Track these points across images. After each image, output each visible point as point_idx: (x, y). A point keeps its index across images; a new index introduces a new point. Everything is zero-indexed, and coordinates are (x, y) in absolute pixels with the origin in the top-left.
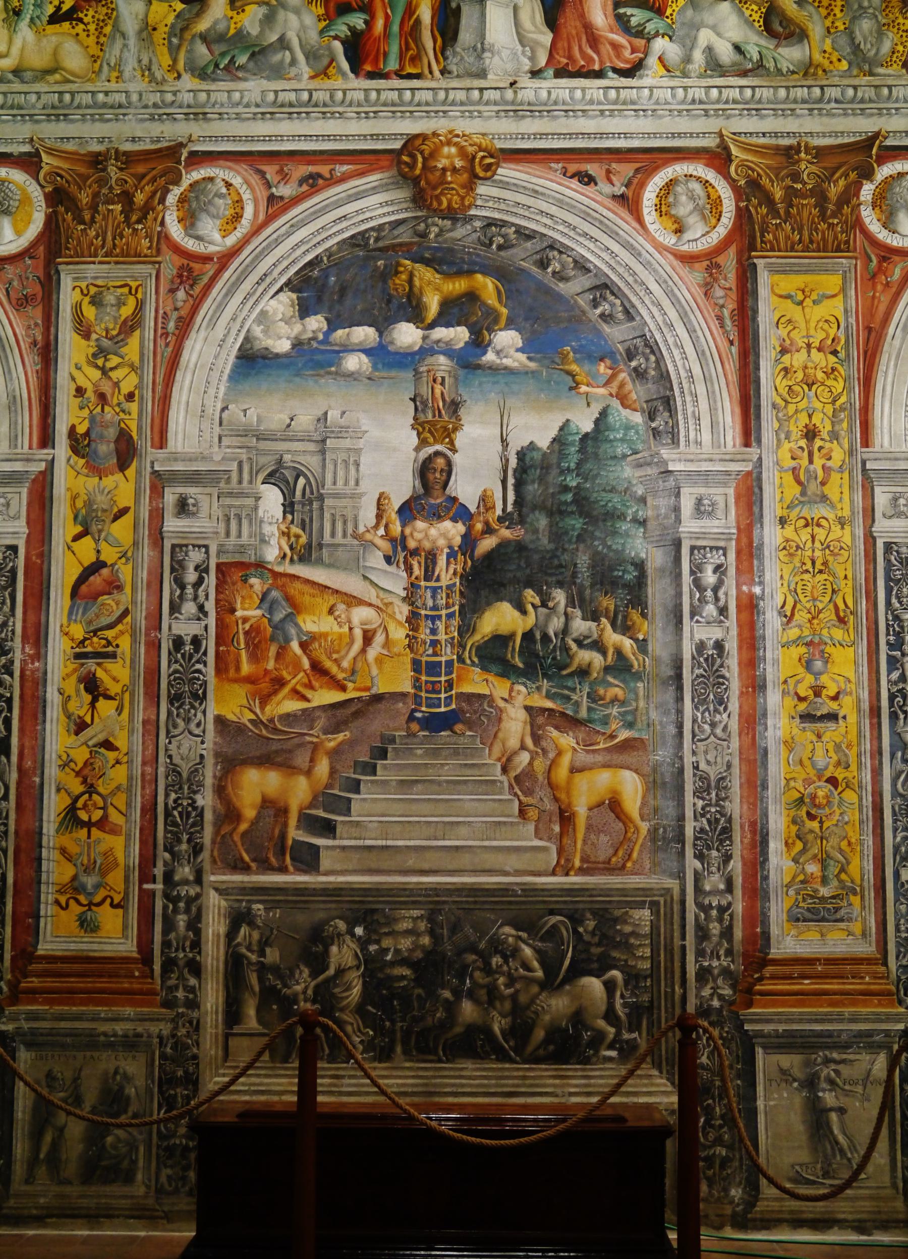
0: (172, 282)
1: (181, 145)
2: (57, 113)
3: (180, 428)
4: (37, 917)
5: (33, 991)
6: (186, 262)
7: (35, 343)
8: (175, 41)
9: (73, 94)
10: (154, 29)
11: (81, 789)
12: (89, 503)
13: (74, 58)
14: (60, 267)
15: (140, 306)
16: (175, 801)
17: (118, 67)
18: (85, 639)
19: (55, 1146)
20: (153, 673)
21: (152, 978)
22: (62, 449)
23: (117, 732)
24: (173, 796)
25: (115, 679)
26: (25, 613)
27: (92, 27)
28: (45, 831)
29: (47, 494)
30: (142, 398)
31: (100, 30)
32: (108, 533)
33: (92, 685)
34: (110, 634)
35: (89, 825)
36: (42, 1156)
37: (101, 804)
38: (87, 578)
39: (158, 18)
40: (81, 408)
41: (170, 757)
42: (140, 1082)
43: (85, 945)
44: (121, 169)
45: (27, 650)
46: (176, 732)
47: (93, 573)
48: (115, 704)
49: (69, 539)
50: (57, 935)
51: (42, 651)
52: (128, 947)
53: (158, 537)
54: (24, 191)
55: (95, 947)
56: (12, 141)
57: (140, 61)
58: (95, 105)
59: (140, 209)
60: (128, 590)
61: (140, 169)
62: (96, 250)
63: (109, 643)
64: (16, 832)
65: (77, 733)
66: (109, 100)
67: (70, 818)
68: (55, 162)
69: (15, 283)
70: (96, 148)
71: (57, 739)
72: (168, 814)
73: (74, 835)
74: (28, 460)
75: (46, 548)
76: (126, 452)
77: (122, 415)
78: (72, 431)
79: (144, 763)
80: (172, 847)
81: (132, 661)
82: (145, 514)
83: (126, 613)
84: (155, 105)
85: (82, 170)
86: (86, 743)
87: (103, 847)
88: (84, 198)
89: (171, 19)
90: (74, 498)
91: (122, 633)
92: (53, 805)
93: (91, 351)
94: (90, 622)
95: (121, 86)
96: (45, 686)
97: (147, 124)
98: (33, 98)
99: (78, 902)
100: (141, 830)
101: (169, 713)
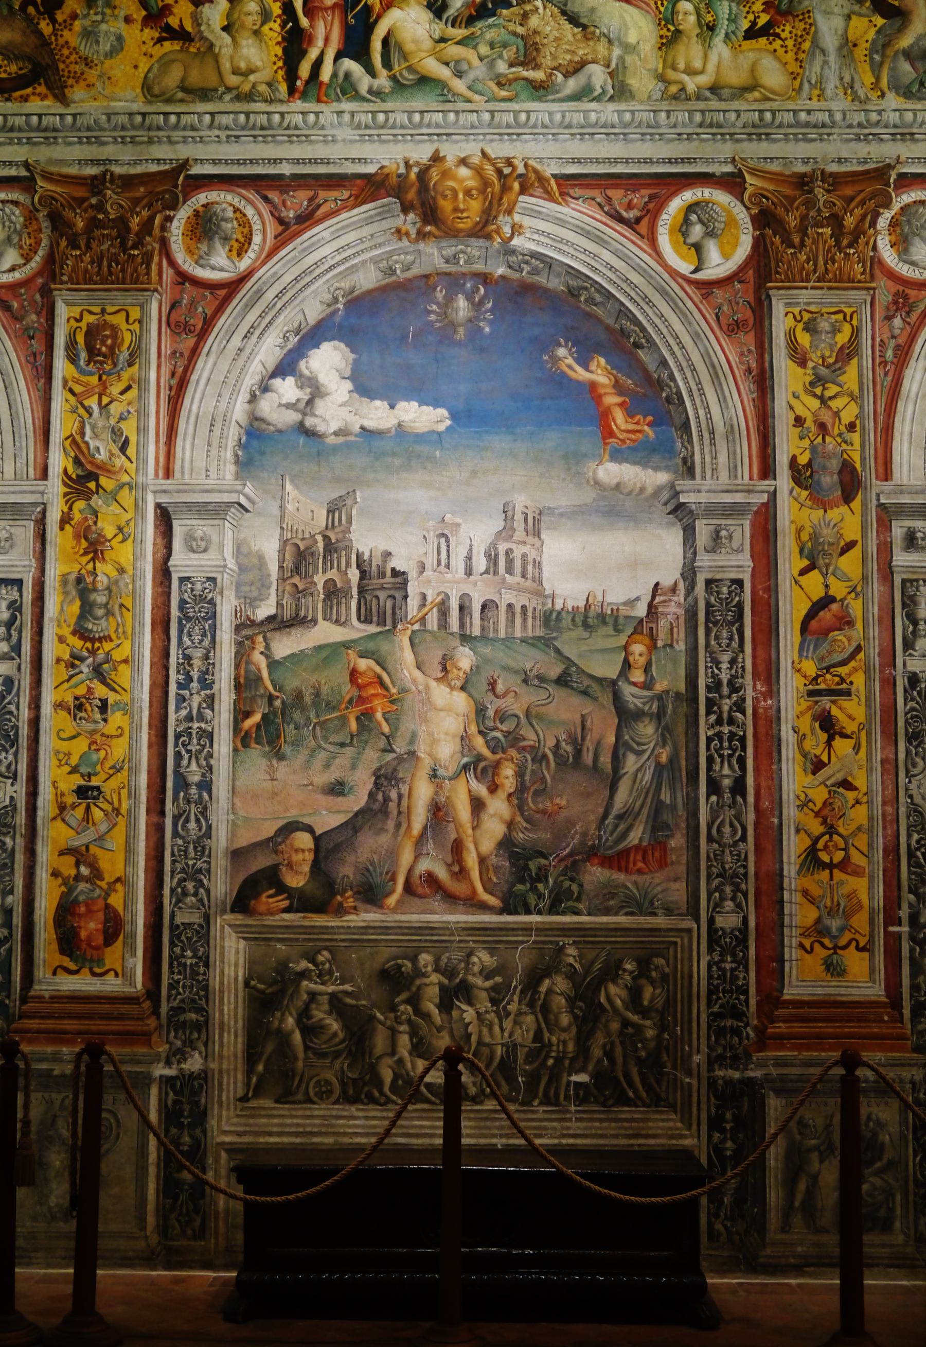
0: (888, 309)
1: (890, 167)
2: (759, 132)
3: (905, 459)
4: (782, 961)
5: (781, 1037)
6: (901, 288)
7: (749, 370)
8: (877, 57)
9: (773, 112)
10: (855, 45)
11: (821, 829)
12: (814, 536)
13: (773, 76)
14: (771, 292)
15: (856, 333)
16: (918, 842)
17: (820, 85)
18: (818, 676)
19: (810, 1194)
20: (889, 711)
21: (902, 1023)
22: (783, 480)
23: (855, 771)
24: (916, 837)
25: (850, 717)
26: (754, 649)
27: (789, 43)
28: (785, 873)
29: (771, 527)
30: (863, 428)
31: (798, 46)
32: (836, 568)
33: (827, 724)
34: (843, 671)
35: (830, 866)
36: (797, 1204)
37: (843, 846)
38: (816, 614)
39: (858, 34)
40: (801, 438)
41: (911, 797)
42: (894, 1129)
43: (833, 989)
44: (828, 191)
45: (759, 687)
46: (916, 771)
47: (823, 608)
48: (852, 742)
49: (796, 573)
50: (803, 979)
51: (775, 689)
52: (876, 991)
53: (887, 571)
54: (729, 213)
55: (843, 991)
56: (713, 161)
57: (842, 79)
58: (798, 124)
59: (851, 233)
60: (859, 625)
61: (849, 191)
62: (808, 275)
63: (843, 680)
64: (756, 874)
65: (814, 773)
66: (813, 118)
67: (812, 860)
68: (760, 183)
69: (725, 308)
70: (801, 168)
71: (794, 779)
72: (911, 855)
73: (816, 876)
74: (749, 491)
75: (772, 582)
76: (850, 484)
77: (844, 446)
78: (793, 460)
79: (884, 803)
80: (917, 889)
81: (868, 699)
82: (873, 548)
83: (858, 649)
84: (860, 125)
85: (788, 191)
86: (824, 783)
87: (845, 890)
88: (792, 220)
89: (871, 35)
90: (799, 531)
91: (855, 670)
92: (793, 846)
93: (808, 379)
94: (822, 659)
95: (823, 105)
96: (779, 724)
97: (853, 144)
98: (733, 116)
99: (822, 945)
100: (884, 871)
101: (908, 752)
